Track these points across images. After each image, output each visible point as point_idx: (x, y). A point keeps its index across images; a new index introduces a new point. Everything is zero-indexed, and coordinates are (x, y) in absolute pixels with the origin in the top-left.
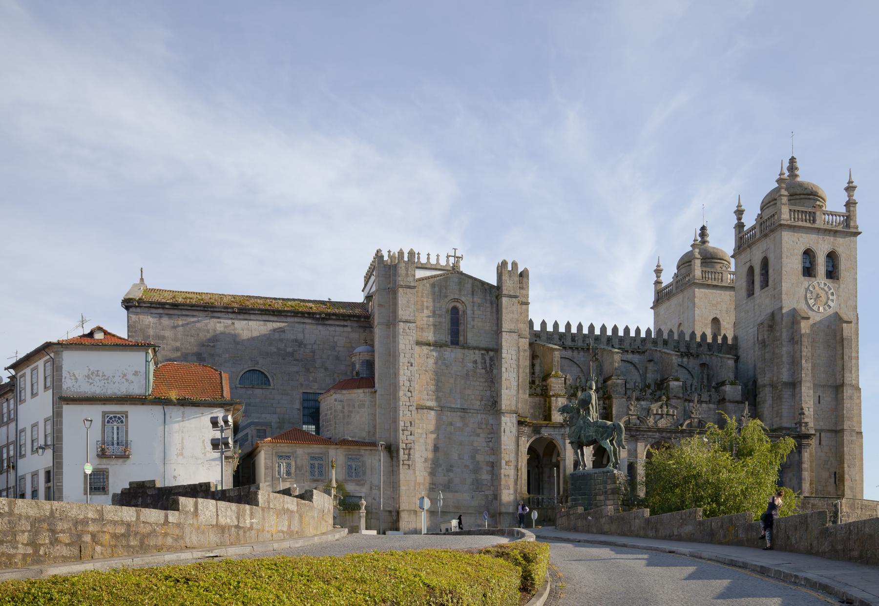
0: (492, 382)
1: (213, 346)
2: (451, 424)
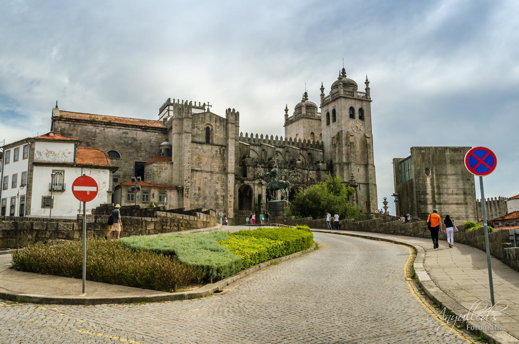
0: (224, 160)
1: (94, 139)
2: (206, 178)
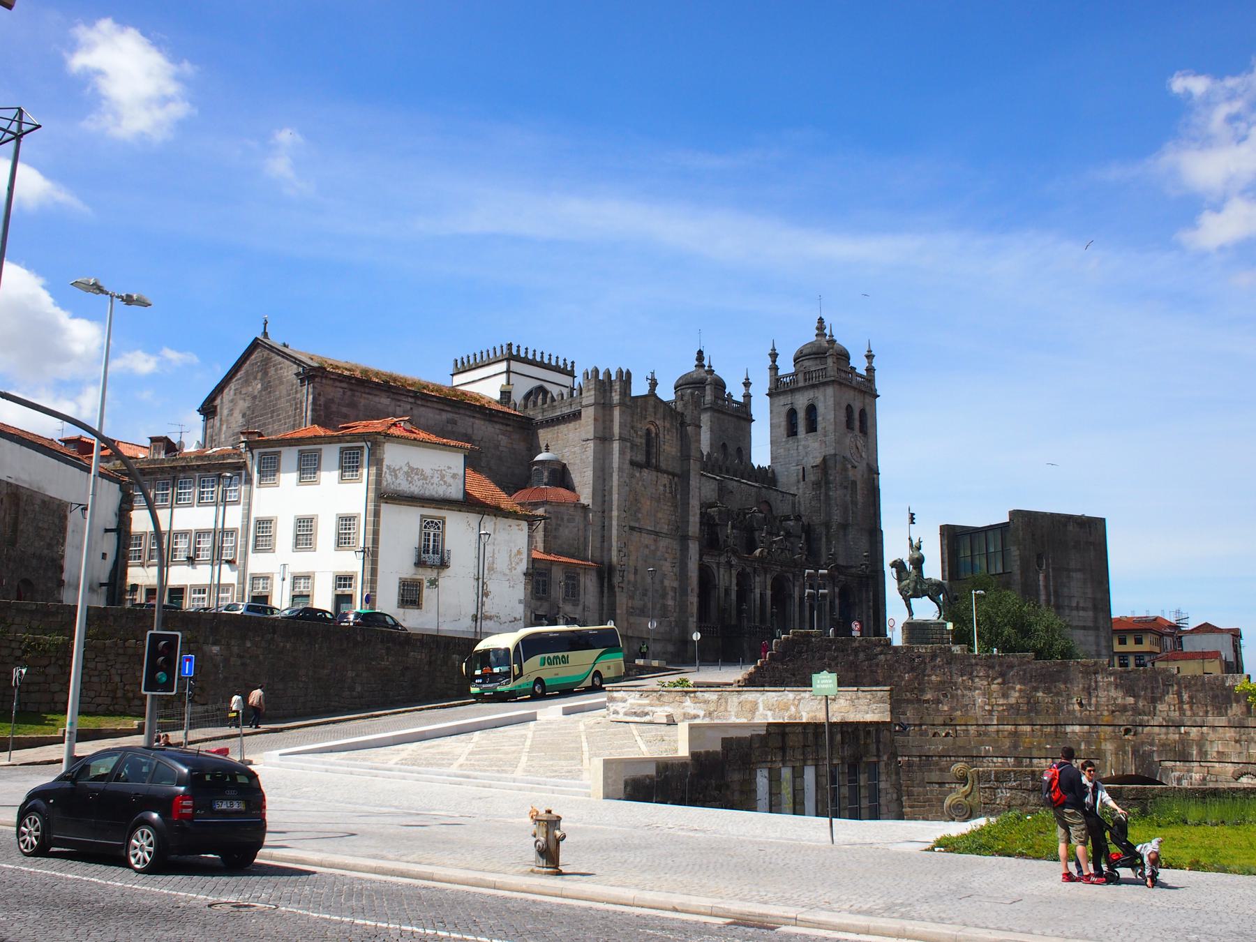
0: (676, 506)
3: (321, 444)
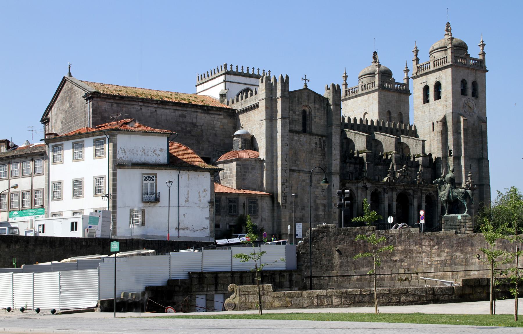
0: (324, 155)
3: (83, 138)
